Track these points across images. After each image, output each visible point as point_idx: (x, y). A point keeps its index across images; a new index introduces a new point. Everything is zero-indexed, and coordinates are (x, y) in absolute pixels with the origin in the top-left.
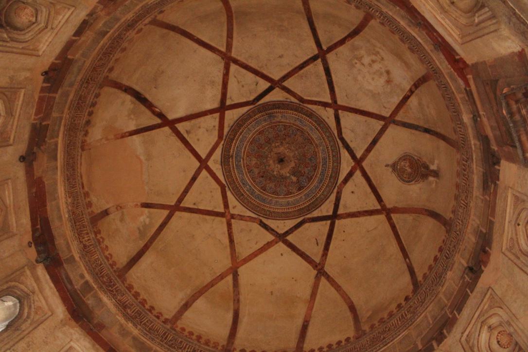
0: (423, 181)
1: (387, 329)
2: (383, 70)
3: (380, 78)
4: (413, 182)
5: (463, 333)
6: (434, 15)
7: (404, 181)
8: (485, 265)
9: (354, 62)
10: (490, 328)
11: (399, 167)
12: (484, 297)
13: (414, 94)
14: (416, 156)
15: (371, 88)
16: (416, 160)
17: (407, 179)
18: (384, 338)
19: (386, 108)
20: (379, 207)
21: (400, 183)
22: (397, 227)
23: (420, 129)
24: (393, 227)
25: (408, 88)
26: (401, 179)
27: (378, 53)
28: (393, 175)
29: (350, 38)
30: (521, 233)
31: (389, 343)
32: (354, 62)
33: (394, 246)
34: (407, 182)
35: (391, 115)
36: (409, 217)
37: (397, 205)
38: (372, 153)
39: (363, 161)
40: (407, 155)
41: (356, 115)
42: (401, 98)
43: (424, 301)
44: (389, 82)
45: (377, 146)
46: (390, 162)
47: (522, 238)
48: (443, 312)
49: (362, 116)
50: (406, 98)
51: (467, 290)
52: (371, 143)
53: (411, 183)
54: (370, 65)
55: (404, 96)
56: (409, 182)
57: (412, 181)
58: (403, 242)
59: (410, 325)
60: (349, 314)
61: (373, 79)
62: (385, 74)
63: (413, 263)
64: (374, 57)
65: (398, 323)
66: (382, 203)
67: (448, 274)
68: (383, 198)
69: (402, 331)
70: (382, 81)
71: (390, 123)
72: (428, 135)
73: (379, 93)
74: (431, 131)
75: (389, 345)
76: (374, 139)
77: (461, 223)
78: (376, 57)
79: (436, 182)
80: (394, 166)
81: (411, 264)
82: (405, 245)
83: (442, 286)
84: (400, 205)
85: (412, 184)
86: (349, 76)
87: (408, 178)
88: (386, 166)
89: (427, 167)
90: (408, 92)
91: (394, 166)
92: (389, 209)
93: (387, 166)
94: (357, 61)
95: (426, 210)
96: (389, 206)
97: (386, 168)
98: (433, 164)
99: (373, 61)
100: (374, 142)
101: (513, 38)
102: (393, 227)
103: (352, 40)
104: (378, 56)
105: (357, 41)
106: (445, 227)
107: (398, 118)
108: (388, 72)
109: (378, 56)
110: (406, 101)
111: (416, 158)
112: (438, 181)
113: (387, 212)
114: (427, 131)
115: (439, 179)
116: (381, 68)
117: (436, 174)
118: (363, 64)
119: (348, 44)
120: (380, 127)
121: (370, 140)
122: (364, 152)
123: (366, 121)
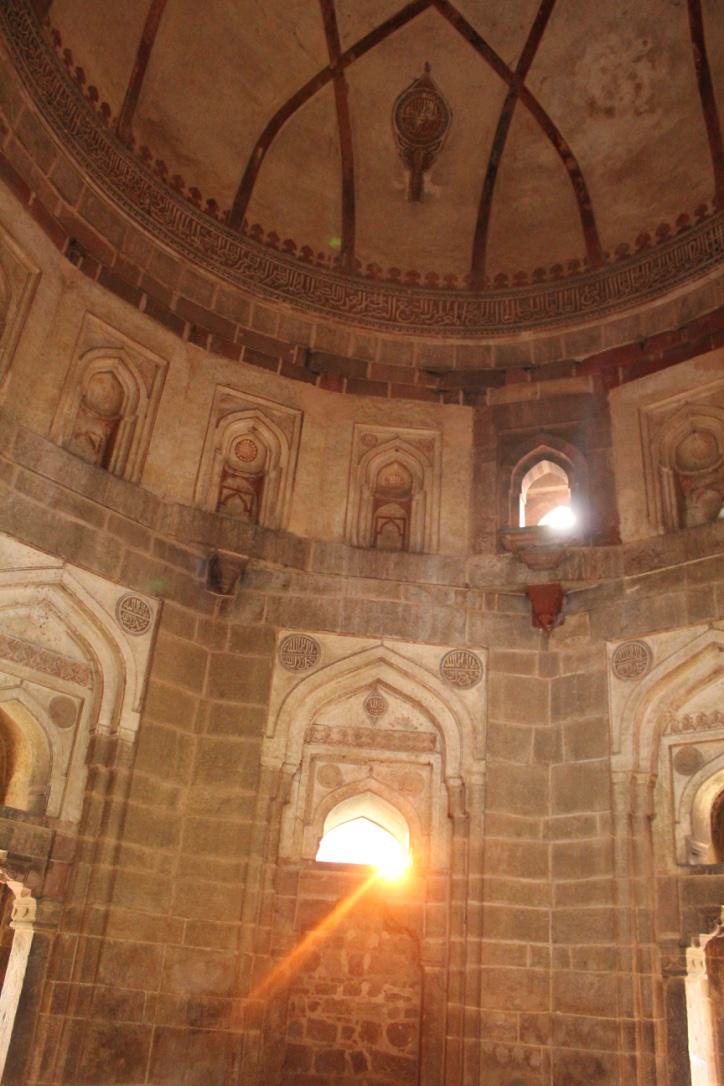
0: (400, 155)
1: (162, 205)
2: (616, 103)
3: (603, 88)
4: (397, 131)
5: (228, 385)
6: (687, 390)
7: (398, 109)
8: (325, 385)
9: (650, 40)
10: (254, 429)
11: (424, 95)
12: (287, 406)
13: (560, 160)
14: (446, 139)
15: (588, 59)
16: (438, 137)
17: (402, 115)
18: (149, 213)
19: (542, 83)
20: (344, 48)
21: (393, 98)
22: (311, 100)
23: (495, 156)
24: (308, 91)
25: (575, 150)
26: (404, 100)
27: (652, 111)
28: (410, 82)
29: (698, 60)
30: (387, 457)
31: (149, 231)
32: (650, 40)
33: (275, 102)
34: (397, 115)
35: (525, 91)
36: (330, 128)
37: (351, 89)
38: (454, 31)
39: (439, 9)
40: (447, 115)
41: (538, 7)
42: (557, 124)
43: (230, 262)
44: (592, 104)
45: (469, 49)
46: (434, 76)
47: (382, 459)
48: (233, 322)
49: (533, 21)
50: (554, 136)
51: (281, 362)
52: (475, 33)
53: (396, 127)
54: (633, 76)
55: (560, 136)
56: (397, 119)
57: (399, 127)
58: (286, 124)
59: (190, 260)
60: (133, 52)
61: (604, 71)
62: (608, 104)
63: (261, 170)
64: (646, 93)
65: (178, 225)
66: (352, 57)
67: (285, 305)
68: (364, 59)
69: (174, 246)
70: (597, 92)
71: (511, 86)
72: (483, 172)
73: (574, 74)
74: (491, 187)
75: (146, 233)
76: (485, 43)
77: (363, 306)
78: (644, 100)
79: (403, 191)
80: (425, 85)
81: (259, 167)
82: (280, 131)
83: (265, 299)
84: (351, 100)
85: (393, 129)
86: (625, 13)
87: (404, 119)
88: (427, 64)
89: (426, 166)
90: (567, 147)
91: (425, 85)
92: (342, 74)
93: (427, 68)
94: (650, 46)
95: (351, 170)
96: (348, 71)
97: (423, 65)
98: (434, 181)
99: (638, 87)
100: (477, 42)
101: (636, 538)
102: (308, 91)
103: (693, 64)
104: (647, 107)
105: (687, 75)
106: (342, 252)
107: (520, 109)
108: (609, 112)
109: (647, 107)
110: (549, 135)
111: (442, 138)
112: (406, 198)
113: (335, 72)
114: (492, 171)
115: (409, 200)
116: (621, 99)
117: (417, 193)
118: (638, 59)
119: (688, 48)
120: (506, 59)
121: (482, 31)
122: (459, 14)
123: (522, 27)
